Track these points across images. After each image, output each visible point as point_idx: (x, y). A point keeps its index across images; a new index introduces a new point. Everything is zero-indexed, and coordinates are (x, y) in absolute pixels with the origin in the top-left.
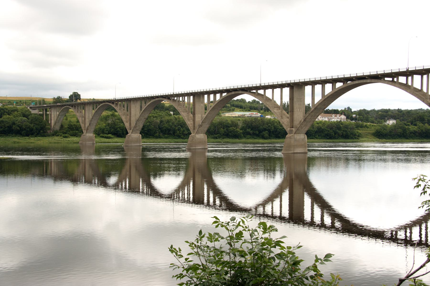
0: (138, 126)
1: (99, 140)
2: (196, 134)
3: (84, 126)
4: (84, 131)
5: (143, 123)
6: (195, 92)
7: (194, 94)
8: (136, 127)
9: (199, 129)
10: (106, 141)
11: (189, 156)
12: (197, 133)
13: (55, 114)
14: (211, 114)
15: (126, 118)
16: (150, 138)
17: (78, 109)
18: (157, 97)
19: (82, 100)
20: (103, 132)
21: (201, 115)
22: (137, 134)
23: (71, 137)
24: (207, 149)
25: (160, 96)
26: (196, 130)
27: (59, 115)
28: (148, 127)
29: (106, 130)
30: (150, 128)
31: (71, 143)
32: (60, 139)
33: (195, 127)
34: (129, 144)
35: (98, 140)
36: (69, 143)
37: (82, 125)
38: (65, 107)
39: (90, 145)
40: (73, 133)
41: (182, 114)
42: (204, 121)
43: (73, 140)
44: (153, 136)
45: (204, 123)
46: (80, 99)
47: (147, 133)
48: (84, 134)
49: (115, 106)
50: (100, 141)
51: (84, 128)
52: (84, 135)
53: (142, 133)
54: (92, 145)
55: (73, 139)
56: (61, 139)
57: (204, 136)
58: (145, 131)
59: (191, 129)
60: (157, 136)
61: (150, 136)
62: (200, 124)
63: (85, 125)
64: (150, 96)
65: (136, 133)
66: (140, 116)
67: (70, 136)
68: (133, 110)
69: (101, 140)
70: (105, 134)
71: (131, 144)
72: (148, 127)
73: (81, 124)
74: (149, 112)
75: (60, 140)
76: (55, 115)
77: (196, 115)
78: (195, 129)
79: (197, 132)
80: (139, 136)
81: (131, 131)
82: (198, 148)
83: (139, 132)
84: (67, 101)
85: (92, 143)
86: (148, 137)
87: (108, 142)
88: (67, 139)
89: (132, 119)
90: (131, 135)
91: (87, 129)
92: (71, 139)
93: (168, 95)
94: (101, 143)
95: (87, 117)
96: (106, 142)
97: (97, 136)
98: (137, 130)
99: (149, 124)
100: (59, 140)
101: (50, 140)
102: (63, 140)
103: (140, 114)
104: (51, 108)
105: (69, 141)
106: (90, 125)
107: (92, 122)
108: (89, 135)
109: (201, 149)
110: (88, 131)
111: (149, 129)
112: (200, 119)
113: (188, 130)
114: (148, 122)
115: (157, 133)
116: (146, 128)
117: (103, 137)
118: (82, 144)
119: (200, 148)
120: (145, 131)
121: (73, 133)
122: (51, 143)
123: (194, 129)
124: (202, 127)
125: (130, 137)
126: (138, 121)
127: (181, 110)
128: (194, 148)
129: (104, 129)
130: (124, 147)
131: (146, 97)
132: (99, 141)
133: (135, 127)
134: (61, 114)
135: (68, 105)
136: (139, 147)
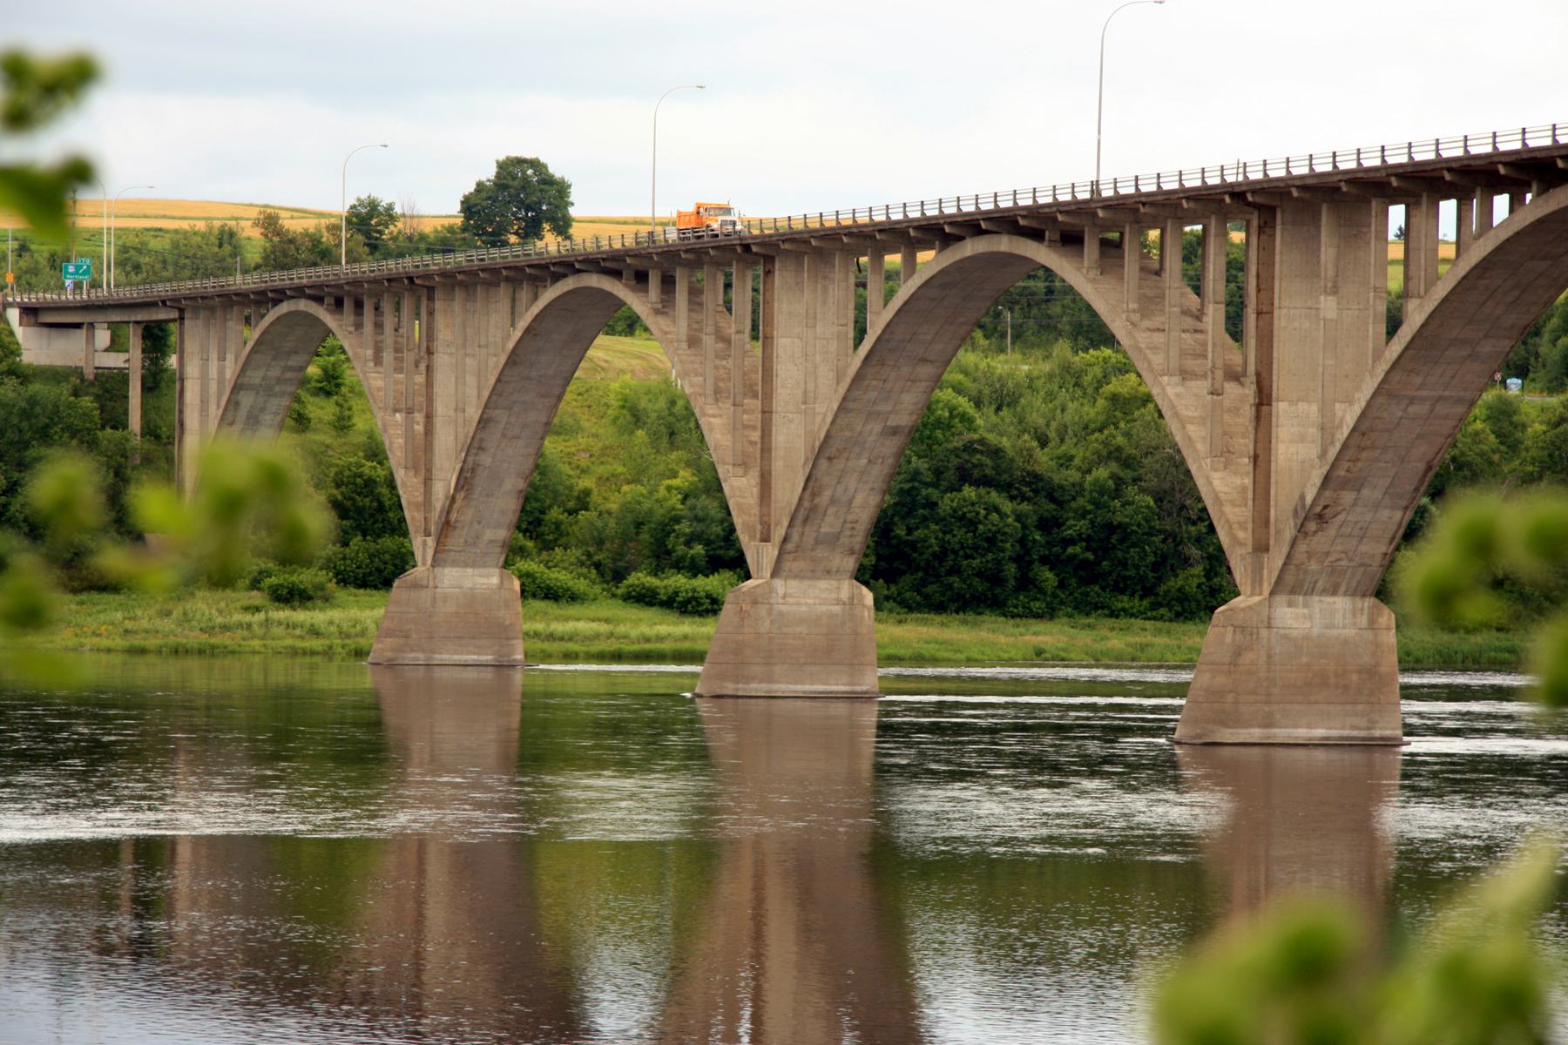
0: (833, 501)
1: (604, 628)
2: (1281, 599)
3: (421, 499)
4: (421, 546)
5: (879, 473)
6: (1412, 162)
7: (1260, 199)
8: (813, 509)
9: (1302, 547)
10: (660, 639)
11: (1217, 820)
12: (1290, 584)
13: (213, 371)
14: (1412, 401)
15: (736, 427)
16: (1114, 614)
17: (379, 326)
18: (1007, 221)
19: (583, 237)
20: (662, 558)
21: (1322, 411)
22: (823, 584)
23: (342, 594)
24: (1390, 744)
25: (990, 217)
26: (1276, 560)
27: (237, 388)
28: (1098, 505)
29: (685, 527)
30: (1119, 518)
31: (328, 653)
32: (238, 617)
33: (1267, 522)
34: (749, 679)
35: (595, 626)
36: (313, 653)
37: (408, 489)
38: (284, 308)
39: (470, 674)
40: (371, 556)
41: (1170, 391)
42: (1341, 472)
43: (356, 623)
44: (1147, 592)
45: (1344, 485)
46: (562, 226)
47: (1085, 564)
48: (419, 572)
49: (657, 312)
50: (611, 635)
51: (419, 516)
52: (417, 586)
53: (1044, 560)
54: (488, 675)
55: (354, 613)
56: (248, 618)
57: (1363, 621)
58: (1071, 541)
59: (1237, 542)
60: (1183, 597)
61: (1119, 589)
62: (1309, 499)
63: (428, 481)
64: (1452, 151)
65: (813, 575)
66: (842, 408)
67: (331, 586)
68: (786, 344)
69: (621, 629)
70: (678, 566)
71: (770, 680)
72: (1098, 505)
73: (400, 475)
74: (926, 371)
75: (240, 625)
76: (213, 387)
77: (1281, 408)
78: (1267, 549)
79: (1290, 579)
80: (852, 601)
81: (770, 552)
82: (1302, 733)
83: (850, 563)
84: (444, 244)
85: (488, 658)
86: (1096, 607)
87: (686, 645)
88: (301, 616)
89: (780, 437)
90: (771, 590)
91: (447, 526)
92: (335, 614)
93: (1183, 189)
94: (618, 657)
95: (442, 409)
96: (666, 646)
97: (597, 589)
98: (832, 540)
99: (1113, 476)
100: (225, 628)
101: (145, 624)
102: (267, 623)
103: (842, 390)
104: (182, 318)
105: (315, 632)
106: (465, 481)
107: (486, 459)
108: (468, 584)
109: (1324, 745)
110: (456, 540)
111: (1111, 528)
112: (1310, 451)
113: (1217, 561)
114: (1101, 460)
115: (1186, 561)
116: (1084, 514)
117: (645, 598)
118: (391, 666)
119: (1319, 733)
120: (1071, 541)
121: (371, 556)
122: (143, 651)
123: (1261, 547)
124: (1332, 531)
125: (762, 610)
126: (824, 452)
127: (1157, 360)
128: (1255, 734)
129: (665, 528)
130: (703, 707)
131: (811, 234)
132: (597, 636)
133: (805, 512)
134: (255, 377)
135: (299, 292)
136: (840, 708)
